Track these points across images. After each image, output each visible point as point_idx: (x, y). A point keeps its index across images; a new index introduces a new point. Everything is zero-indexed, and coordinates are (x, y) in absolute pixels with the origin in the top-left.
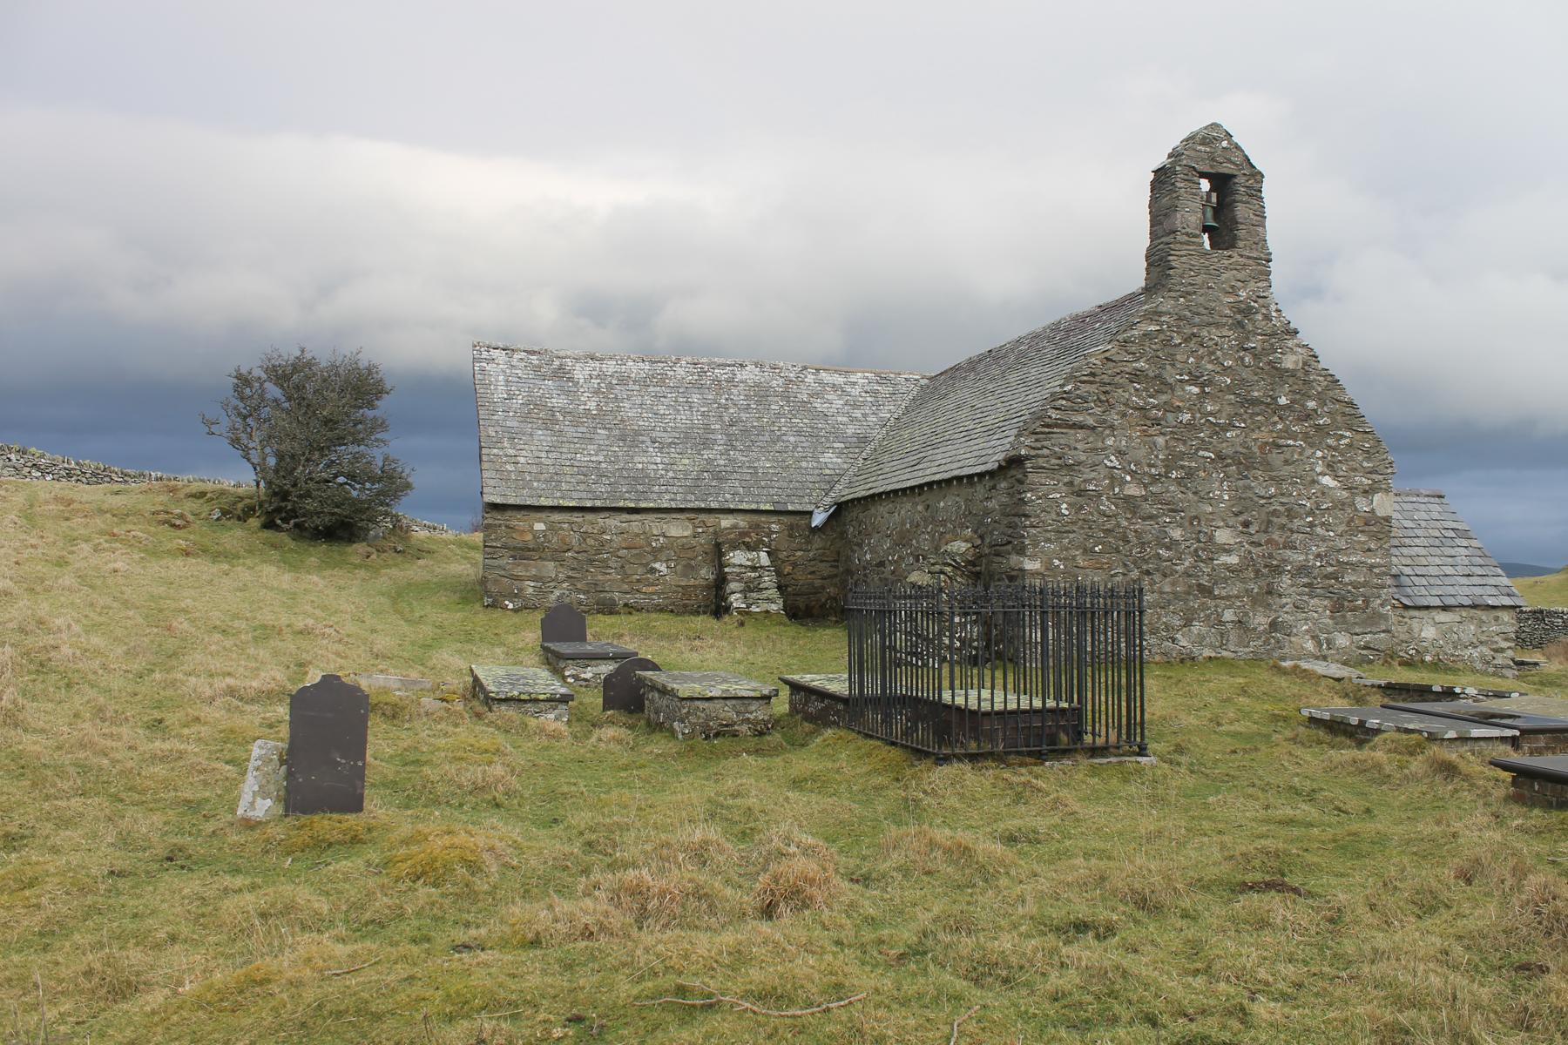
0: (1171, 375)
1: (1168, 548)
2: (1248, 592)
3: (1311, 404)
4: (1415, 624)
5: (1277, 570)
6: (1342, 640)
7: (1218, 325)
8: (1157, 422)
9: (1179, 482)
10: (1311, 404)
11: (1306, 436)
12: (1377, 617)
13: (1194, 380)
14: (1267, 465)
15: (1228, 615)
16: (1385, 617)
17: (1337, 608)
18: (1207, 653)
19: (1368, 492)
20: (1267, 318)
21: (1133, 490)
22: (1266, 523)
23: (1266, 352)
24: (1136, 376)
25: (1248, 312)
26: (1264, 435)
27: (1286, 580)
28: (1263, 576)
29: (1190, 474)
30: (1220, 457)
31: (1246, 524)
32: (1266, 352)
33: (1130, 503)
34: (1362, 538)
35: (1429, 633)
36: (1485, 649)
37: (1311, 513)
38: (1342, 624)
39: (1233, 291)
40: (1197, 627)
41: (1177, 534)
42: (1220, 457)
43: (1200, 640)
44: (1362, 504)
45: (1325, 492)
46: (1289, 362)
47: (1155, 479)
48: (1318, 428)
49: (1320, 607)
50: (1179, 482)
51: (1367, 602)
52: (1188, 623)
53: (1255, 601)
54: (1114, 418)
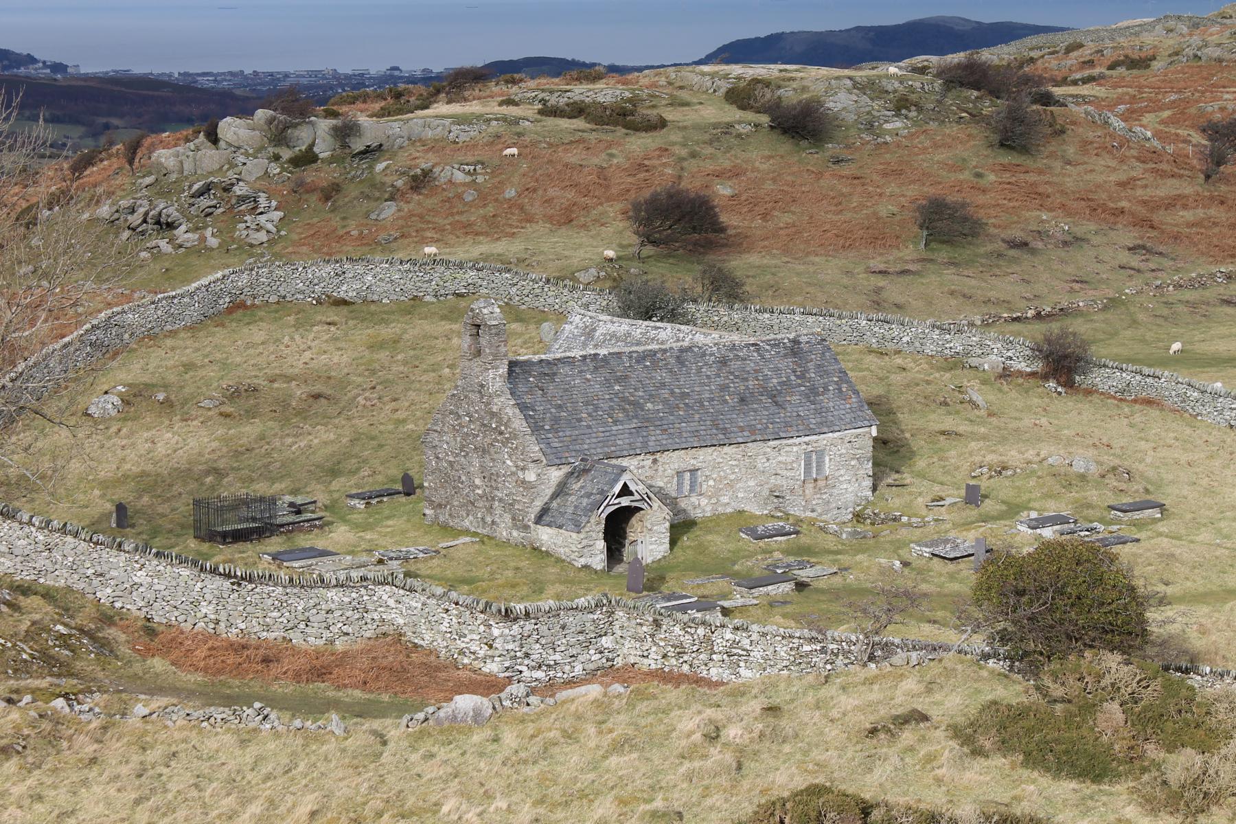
0: (461, 412)
6: (515, 533)
12: (526, 527)
13: (467, 415)
17: (514, 519)
21: (451, 459)
22: (490, 477)
25: (482, 386)
26: (488, 440)
33: (451, 464)
35: (545, 537)
38: (515, 526)
40: (471, 518)
44: (520, 473)
49: (508, 517)
54: (446, 429)
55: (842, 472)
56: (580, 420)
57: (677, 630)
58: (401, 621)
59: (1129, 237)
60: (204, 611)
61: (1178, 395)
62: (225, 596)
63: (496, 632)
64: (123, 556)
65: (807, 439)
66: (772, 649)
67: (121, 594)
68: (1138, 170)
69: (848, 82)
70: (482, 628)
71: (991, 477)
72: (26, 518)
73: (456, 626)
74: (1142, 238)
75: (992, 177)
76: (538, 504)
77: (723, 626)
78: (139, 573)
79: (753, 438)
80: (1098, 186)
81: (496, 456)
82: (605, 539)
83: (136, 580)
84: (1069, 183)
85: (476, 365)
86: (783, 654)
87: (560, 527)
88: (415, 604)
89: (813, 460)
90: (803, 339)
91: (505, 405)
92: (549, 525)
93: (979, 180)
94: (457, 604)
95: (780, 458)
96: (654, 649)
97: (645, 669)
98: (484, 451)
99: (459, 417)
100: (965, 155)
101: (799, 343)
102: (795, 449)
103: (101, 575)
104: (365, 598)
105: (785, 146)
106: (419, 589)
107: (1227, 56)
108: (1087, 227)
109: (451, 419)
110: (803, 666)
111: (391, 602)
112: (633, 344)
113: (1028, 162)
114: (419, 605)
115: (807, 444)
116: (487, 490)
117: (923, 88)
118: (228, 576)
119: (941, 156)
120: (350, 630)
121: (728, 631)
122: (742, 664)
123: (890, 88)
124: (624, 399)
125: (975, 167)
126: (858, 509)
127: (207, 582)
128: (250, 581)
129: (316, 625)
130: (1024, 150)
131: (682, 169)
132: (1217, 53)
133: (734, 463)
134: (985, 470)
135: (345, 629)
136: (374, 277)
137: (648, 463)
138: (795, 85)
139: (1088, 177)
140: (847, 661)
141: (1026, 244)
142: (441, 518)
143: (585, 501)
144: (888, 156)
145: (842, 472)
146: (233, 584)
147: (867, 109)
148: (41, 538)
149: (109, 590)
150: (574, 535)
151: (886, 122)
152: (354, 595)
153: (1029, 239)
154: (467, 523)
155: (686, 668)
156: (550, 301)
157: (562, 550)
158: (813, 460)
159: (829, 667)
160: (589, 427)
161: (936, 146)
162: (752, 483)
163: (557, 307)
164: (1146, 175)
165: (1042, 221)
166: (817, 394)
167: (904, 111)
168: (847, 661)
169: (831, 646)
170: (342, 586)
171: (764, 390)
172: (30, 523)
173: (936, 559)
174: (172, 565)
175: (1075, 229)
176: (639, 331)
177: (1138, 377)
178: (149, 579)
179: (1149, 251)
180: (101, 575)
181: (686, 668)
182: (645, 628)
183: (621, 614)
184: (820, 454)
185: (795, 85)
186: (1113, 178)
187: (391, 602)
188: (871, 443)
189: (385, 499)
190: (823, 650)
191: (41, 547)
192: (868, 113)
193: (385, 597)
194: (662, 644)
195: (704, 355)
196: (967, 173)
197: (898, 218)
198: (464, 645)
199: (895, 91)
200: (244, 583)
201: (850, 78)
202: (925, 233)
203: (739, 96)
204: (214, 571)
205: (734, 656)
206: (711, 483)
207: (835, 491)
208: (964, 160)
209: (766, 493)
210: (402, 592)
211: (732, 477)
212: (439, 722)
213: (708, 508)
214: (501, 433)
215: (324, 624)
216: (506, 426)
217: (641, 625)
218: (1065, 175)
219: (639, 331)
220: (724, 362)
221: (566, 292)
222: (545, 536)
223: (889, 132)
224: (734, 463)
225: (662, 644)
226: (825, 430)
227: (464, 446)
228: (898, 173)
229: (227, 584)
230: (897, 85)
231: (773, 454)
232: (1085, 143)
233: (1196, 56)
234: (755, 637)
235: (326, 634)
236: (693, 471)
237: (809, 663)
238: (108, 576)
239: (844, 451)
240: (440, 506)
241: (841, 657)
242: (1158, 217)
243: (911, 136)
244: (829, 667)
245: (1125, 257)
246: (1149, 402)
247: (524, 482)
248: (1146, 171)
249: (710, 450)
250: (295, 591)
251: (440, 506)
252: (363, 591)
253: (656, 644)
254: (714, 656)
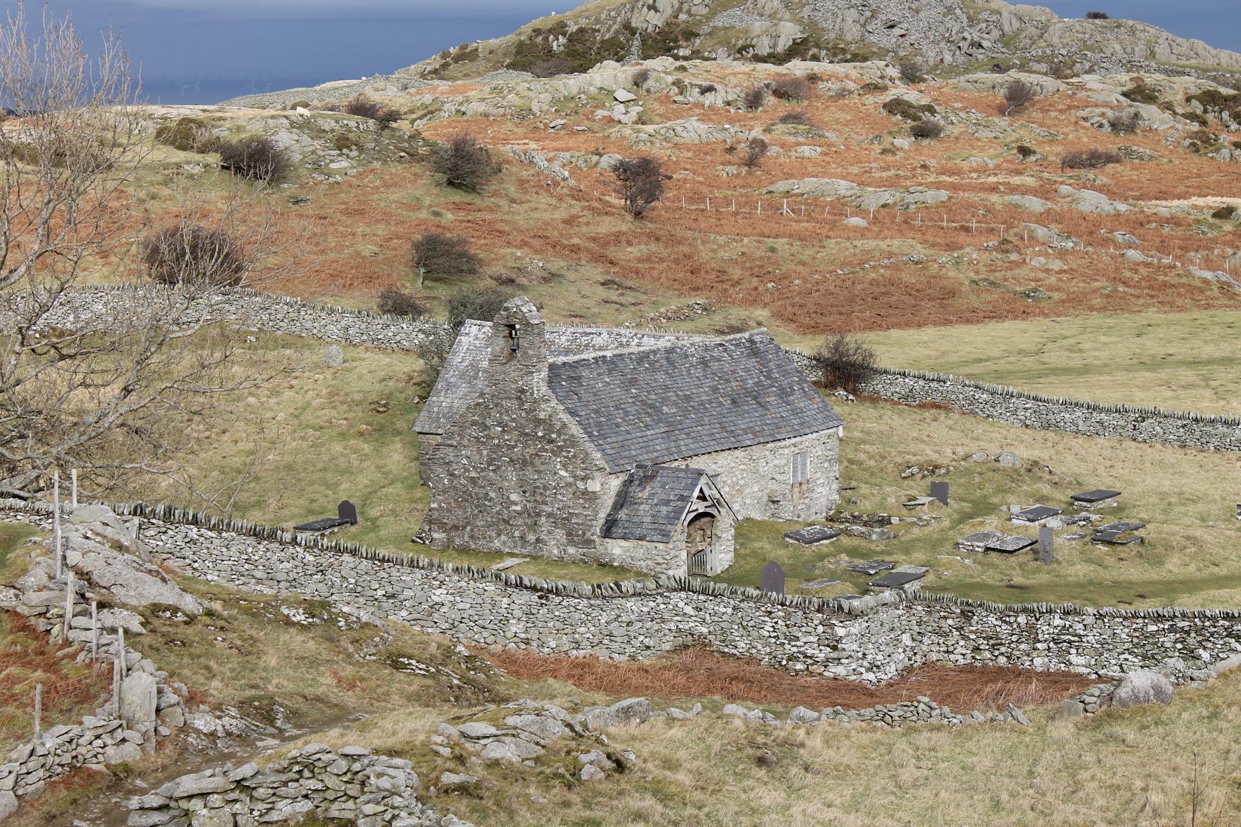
0: (489, 422)
1: (490, 501)
2: (526, 524)
3: (554, 436)
4: (609, 547)
5: (539, 515)
6: (571, 550)
7: (510, 398)
8: (484, 443)
9: (494, 471)
10: (554, 436)
11: (552, 451)
12: (589, 543)
13: (499, 424)
14: (532, 464)
15: (517, 534)
16: (594, 541)
17: (569, 534)
18: (507, 550)
19: (584, 479)
20: (532, 394)
21: (473, 474)
22: (532, 491)
23: (532, 411)
24: (474, 423)
25: (523, 391)
26: (531, 450)
27: (543, 519)
28: (532, 517)
29: (499, 467)
30: (511, 460)
31: (524, 492)
32: (532, 411)
33: (473, 481)
34: (581, 501)
36: (650, 563)
37: (555, 488)
38: (571, 542)
39: (516, 382)
40: (503, 538)
41: (492, 495)
42: (511, 460)
43: (504, 543)
44: (581, 485)
45: (562, 478)
46: (542, 416)
47: (483, 470)
48: (559, 447)
49: (560, 534)
50: (494, 471)
51: (584, 533)
52: (499, 535)
53: (528, 527)
54: (466, 442)
55: (819, 475)
56: (618, 425)
57: (992, 619)
58: (705, 630)
59: (597, 273)
60: (514, 629)
61: (965, 399)
62: (534, 611)
63: (840, 632)
64: (418, 574)
65: (793, 440)
66: (1109, 632)
67: (418, 616)
68: (577, 207)
69: (285, 121)
70: (820, 629)
71: (924, 477)
72: (288, 537)
73: (784, 629)
74: (608, 273)
75: (450, 216)
76: (602, 516)
77: (1050, 612)
78: (438, 592)
79: (757, 440)
80: (547, 223)
81: (542, 468)
83: (436, 599)
84: (520, 220)
85: (513, 370)
86: (1124, 636)
87: (641, 539)
88: (722, 610)
90: (757, 338)
91: (554, 408)
92: (624, 538)
93: (438, 219)
94: (783, 604)
96: (962, 643)
97: (950, 665)
98: (525, 463)
99: (486, 427)
100: (418, 193)
101: (755, 343)
102: (786, 451)
103: (393, 596)
104: (662, 606)
105: (241, 184)
106: (727, 593)
107: (493, 111)
108: (557, 264)
109: (473, 431)
110: (1147, 648)
111: (689, 610)
112: (560, 353)
113: (477, 200)
114: (730, 610)
116: (529, 505)
117: (358, 127)
118: (534, 589)
119: (396, 195)
120: (652, 644)
121: (1057, 617)
122: (1073, 651)
123: (327, 128)
124: (643, 403)
125: (430, 206)
126: (832, 512)
127: (514, 597)
128: (557, 594)
129: (618, 639)
130: (473, 189)
131: (146, 210)
132: (482, 107)
133: (743, 467)
134: (915, 470)
135: (647, 641)
136: (105, 304)
138: (228, 124)
139: (535, 215)
140: (1200, 638)
141: (513, 281)
142: (458, 541)
143: (664, 509)
144: (343, 195)
146: (540, 597)
147: (311, 148)
148: (312, 558)
149: (404, 613)
150: (661, 546)
151: (332, 161)
152: (652, 604)
153: (514, 276)
154: (497, 544)
155: (1002, 660)
156: (308, 325)
157: (643, 564)
159: (1179, 646)
160: (628, 432)
161: (387, 186)
163: (315, 331)
164: (585, 212)
165: (518, 258)
166: (788, 395)
167: (345, 151)
168: (1200, 638)
169: (1181, 624)
170: (640, 594)
171: (748, 393)
172: (294, 542)
173: (993, 554)
174: (475, 581)
175: (549, 266)
176: (563, 338)
177: (921, 382)
178: (451, 598)
179: (620, 286)
180: (393, 596)
181: (1002, 660)
182: (950, 622)
183: (920, 608)
185: (228, 124)
186: (558, 215)
187: (689, 610)
189: (336, 530)
190: (1173, 629)
191: (312, 570)
192: (313, 152)
193: (681, 604)
194: (973, 636)
195: (687, 356)
196: (425, 211)
197: (381, 257)
198: (795, 649)
199: (332, 131)
200: (551, 596)
201: (286, 117)
202: (422, 270)
203: (181, 136)
204: (520, 585)
205: (1063, 643)
207: (814, 495)
208: (417, 199)
209: (765, 499)
210: (702, 597)
211: (742, 482)
212: (1123, 703)
214: (551, 441)
215: (626, 638)
216: (559, 436)
217: (945, 618)
218: (514, 213)
219: (563, 338)
220: (704, 363)
221: (323, 315)
222: (617, 549)
223: (338, 171)
224: (743, 467)
225: (973, 636)
226: (807, 430)
227: (494, 459)
228: (361, 213)
229: (535, 597)
230: (333, 124)
231: (770, 457)
232: (522, 182)
233: (458, 111)
234: (1089, 620)
235: (629, 650)
237: (1155, 644)
238: (401, 597)
240: (456, 527)
241: (1193, 635)
242: (612, 252)
243: (360, 175)
244: (1179, 646)
245: (602, 292)
246: (938, 407)
247: (585, 493)
248: (583, 208)
249: (725, 454)
250: (599, 602)
251: (456, 527)
252: (660, 600)
253: (964, 637)
254: (1039, 645)
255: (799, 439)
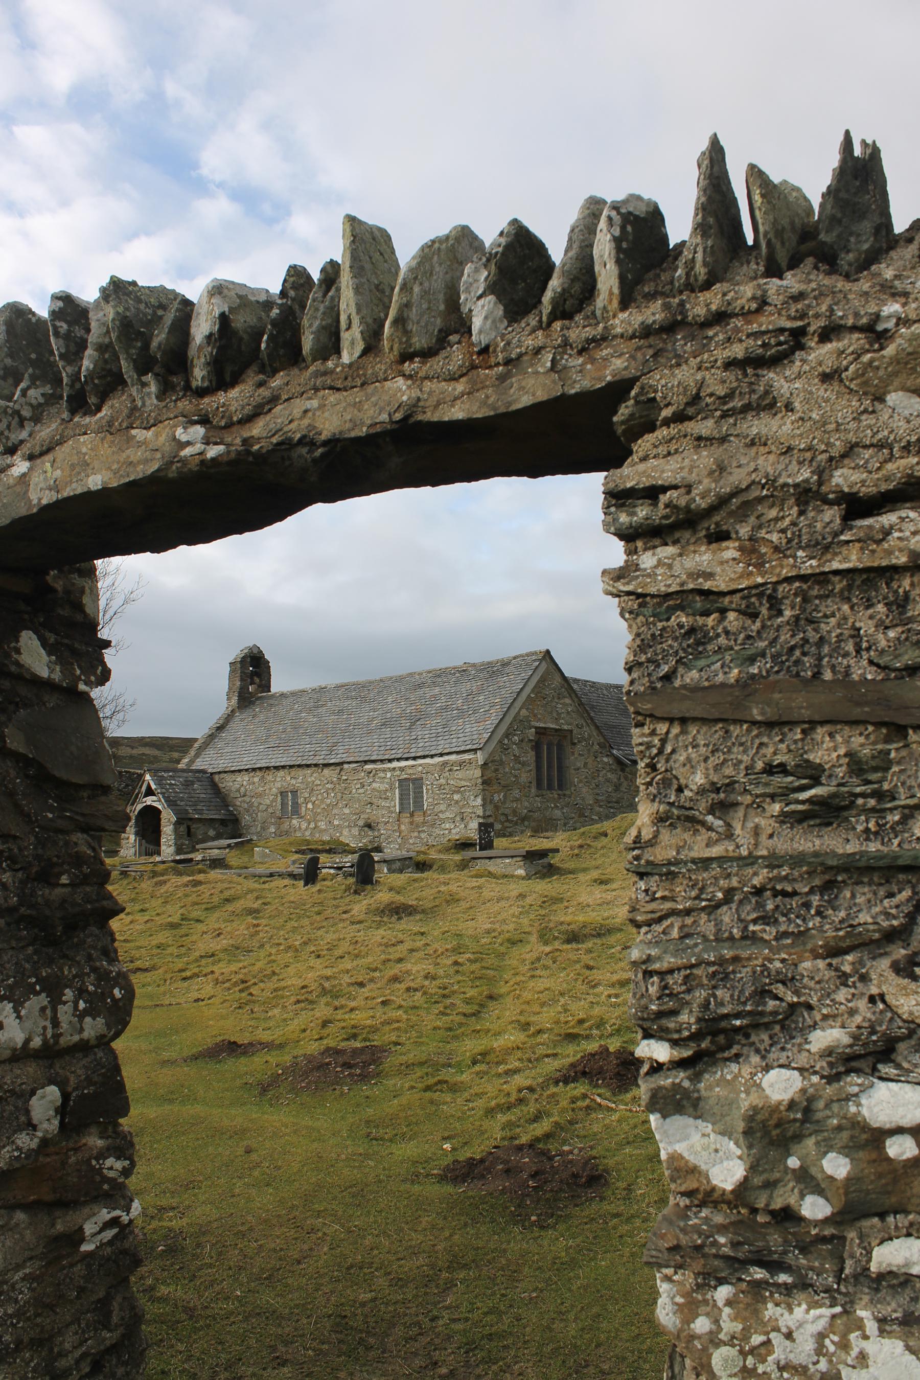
65: (403, 764)
82: (137, 834)
89: (411, 788)
95: (374, 785)
102: (389, 775)
115: (402, 769)
137: (256, 780)
145: (443, 807)
158: (411, 788)
162: (347, 811)
184: (418, 782)
188: (478, 773)
206: (310, 806)
209: (361, 823)
211: (328, 801)
213: (307, 833)
236: (295, 793)
239: (442, 781)
255: (411, 762)
